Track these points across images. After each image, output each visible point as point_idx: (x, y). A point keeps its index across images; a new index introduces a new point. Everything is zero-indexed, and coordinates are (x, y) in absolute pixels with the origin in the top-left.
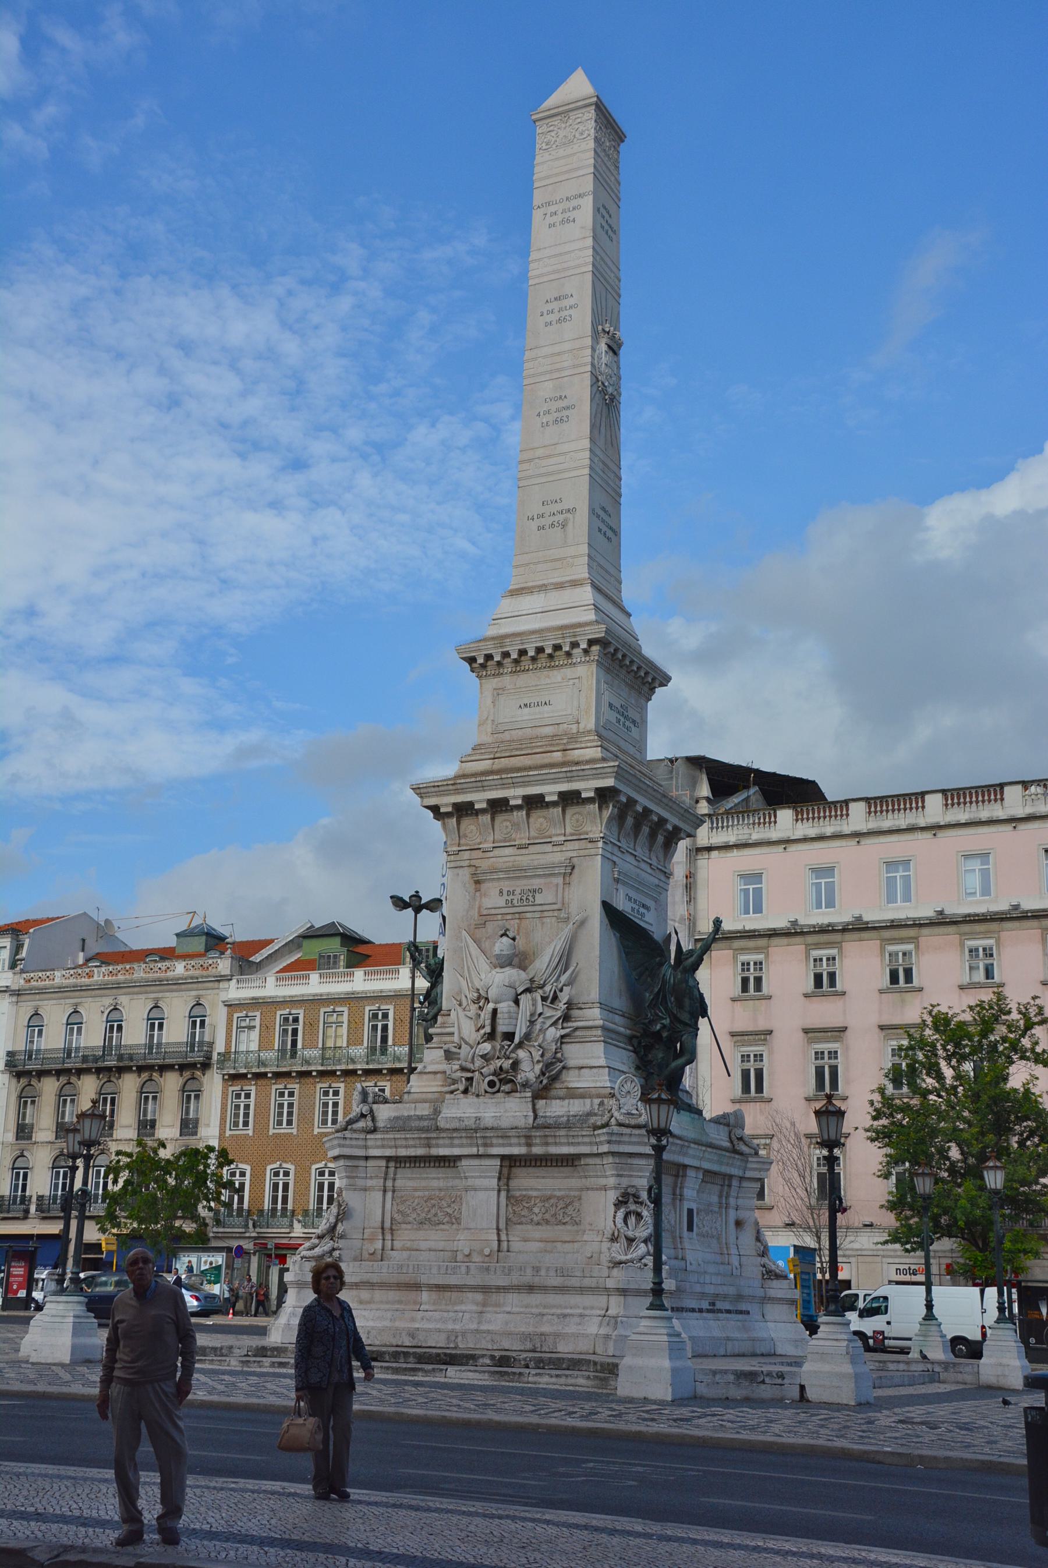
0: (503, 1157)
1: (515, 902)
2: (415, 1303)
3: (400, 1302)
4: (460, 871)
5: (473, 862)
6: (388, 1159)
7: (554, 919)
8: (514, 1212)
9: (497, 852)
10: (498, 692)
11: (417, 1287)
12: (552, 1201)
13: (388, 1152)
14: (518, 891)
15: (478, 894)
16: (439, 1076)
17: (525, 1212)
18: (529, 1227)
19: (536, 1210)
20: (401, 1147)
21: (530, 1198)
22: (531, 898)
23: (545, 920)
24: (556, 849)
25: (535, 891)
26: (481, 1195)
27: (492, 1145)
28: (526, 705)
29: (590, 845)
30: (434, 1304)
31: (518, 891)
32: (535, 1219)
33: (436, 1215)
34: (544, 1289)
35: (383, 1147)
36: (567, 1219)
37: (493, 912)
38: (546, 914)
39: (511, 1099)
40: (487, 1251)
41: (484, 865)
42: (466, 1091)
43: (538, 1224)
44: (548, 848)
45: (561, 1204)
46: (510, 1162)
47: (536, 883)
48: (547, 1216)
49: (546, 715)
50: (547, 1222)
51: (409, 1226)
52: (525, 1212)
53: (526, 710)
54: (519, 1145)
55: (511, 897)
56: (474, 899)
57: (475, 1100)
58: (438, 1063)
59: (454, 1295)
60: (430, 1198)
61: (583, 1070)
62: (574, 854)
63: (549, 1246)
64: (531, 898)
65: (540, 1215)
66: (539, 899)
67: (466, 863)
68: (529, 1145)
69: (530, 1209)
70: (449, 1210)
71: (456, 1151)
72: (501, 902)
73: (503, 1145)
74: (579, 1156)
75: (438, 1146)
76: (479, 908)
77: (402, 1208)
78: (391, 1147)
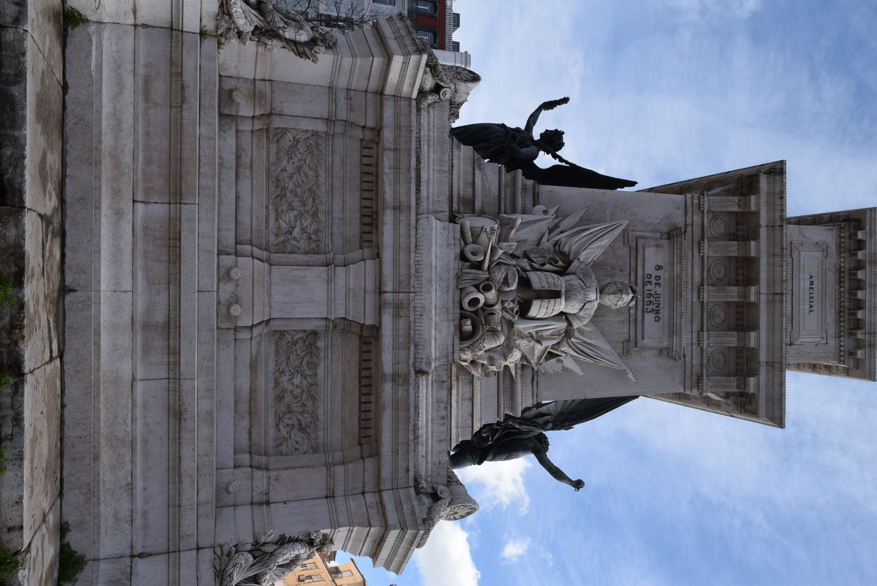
0: (376, 329)
1: (648, 287)
2: (147, 191)
3: (148, 161)
4: (681, 212)
5: (689, 229)
6: (378, 131)
7: (626, 336)
8: (295, 343)
9: (697, 260)
10: (824, 248)
11: (176, 195)
12: (309, 404)
13: (388, 135)
14: (659, 290)
15: (658, 235)
16: (470, 190)
17: (294, 361)
18: (272, 367)
19: (297, 380)
20: (397, 160)
21: (315, 366)
22: (650, 307)
23: (627, 324)
24: (695, 335)
25: (657, 312)
26: (320, 290)
27: (396, 316)
28: (812, 283)
29: (695, 378)
30: (146, 228)
31: (659, 290)
32: (285, 379)
33: (291, 208)
34: (176, 438)
35: (398, 127)
36: (284, 432)
37: (640, 257)
38: (632, 326)
39: (452, 329)
40: (236, 310)
41: (686, 244)
42: (463, 257)
43: (277, 383)
44: (696, 328)
45: (306, 419)
46: (369, 337)
47: (664, 313)
48: (288, 398)
49: (801, 307)
50: (279, 398)
51: (272, 158)
52: (294, 361)
53: (808, 283)
54: (396, 363)
55: (653, 280)
56: (653, 231)
57: (452, 274)
58: (483, 185)
59: (160, 269)
60: (314, 197)
61: (470, 403)
62: (688, 360)
63: (244, 407)
64: (650, 307)
65: (289, 387)
66: (649, 318)
67: (689, 221)
68: (395, 377)
69: (298, 371)
70: (296, 232)
71: (387, 254)
72: (650, 269)
73: (395, 336)
74: (376, 454)
75: (396, 225)
76: (644, 238)
77: (302, 147)
78: (396, 140)
